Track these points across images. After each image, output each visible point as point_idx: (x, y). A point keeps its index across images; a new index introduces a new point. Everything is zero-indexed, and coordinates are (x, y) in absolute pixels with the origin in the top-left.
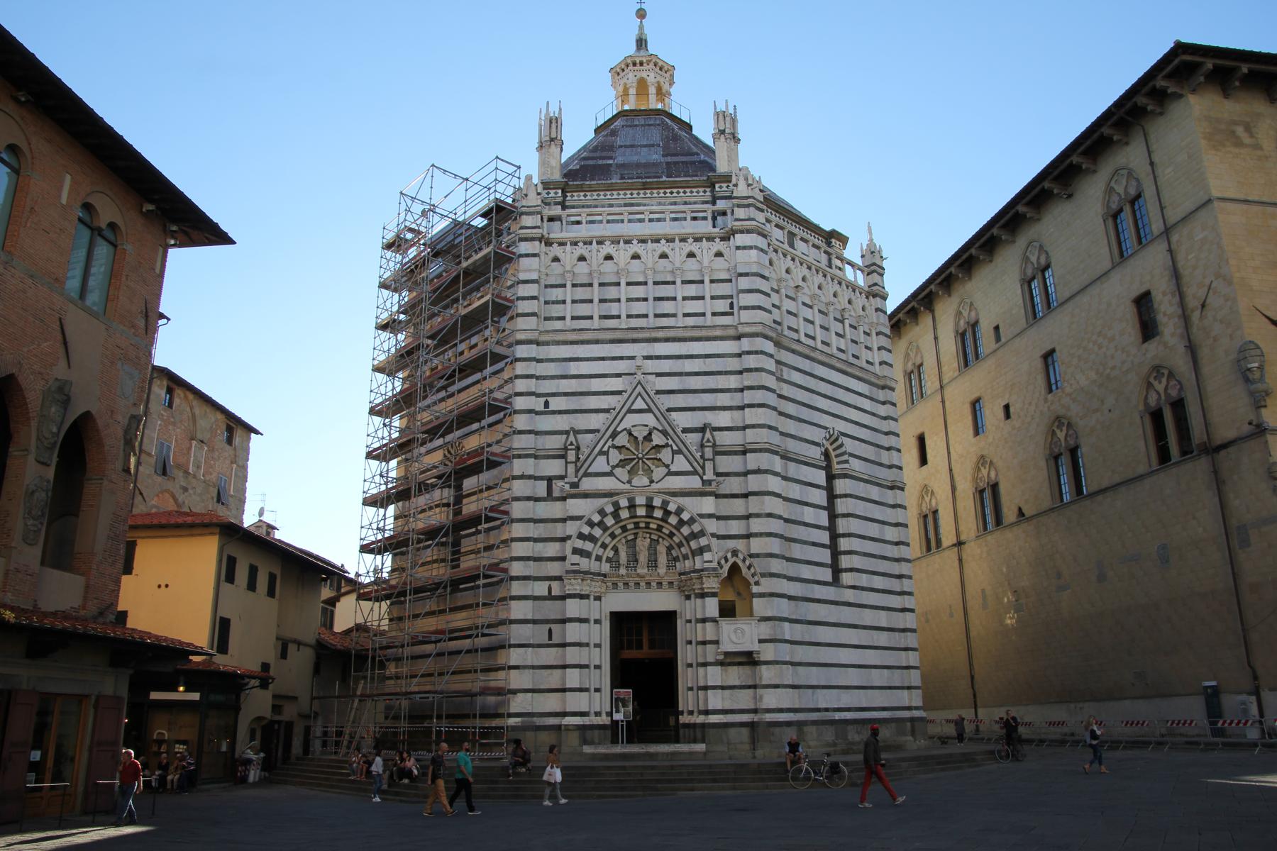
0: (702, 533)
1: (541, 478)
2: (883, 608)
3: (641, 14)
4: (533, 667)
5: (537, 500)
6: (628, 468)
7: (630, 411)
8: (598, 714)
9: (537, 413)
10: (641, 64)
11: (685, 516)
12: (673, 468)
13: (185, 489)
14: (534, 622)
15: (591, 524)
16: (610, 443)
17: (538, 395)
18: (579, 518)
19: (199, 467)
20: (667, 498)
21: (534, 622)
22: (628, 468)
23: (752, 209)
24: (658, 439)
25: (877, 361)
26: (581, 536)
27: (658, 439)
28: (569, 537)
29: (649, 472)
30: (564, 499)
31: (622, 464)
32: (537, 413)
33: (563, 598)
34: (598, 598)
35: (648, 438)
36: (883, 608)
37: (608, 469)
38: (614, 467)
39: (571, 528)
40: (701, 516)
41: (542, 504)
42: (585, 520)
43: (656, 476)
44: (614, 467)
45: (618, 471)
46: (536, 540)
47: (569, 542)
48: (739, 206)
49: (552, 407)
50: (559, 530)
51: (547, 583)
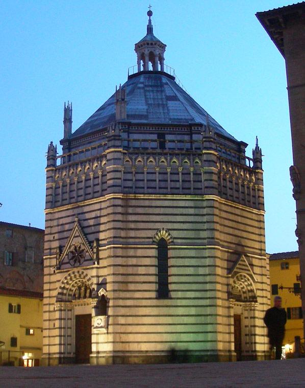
0: (92, 284)
1: (52, 266)
2: (193, 306)
3: (150, 14)
4: (49, 337)
5: (50, 275)
6: (73, 260)
7: (75, 237)
8: (70, 353)
9: (50, 241)
10: (142, 46)
11: (88, 278)
12: (86, 258)
13: (24, 269)
14: (49, 320)
15: (63, 283)
16: (69, 251)
17: (51, 234)
18: (59, 281)
19: (31, 258)
21: (49, 320)
22: (73, 260)
23: (113, 141)
24: (83, 247)
25: (203, 188)
26: (60, 288)
27: (83, 247)
28: (57, 288)
29: (79, 262)
30: (56, 274)
31: (72, 259)
32: (50, 241)
33: (55, 311)
34: (71, 310)
35: (80, 247)
36: (193, 306)
37: (67, 261)
38: (70, 260)
39: (58, 285)
40: (92, 277)
42: (61, 281)
43: (81, 262)
44: (70, 260)
46: (50, 290)
48: (109, 141)
49: (55, 238)
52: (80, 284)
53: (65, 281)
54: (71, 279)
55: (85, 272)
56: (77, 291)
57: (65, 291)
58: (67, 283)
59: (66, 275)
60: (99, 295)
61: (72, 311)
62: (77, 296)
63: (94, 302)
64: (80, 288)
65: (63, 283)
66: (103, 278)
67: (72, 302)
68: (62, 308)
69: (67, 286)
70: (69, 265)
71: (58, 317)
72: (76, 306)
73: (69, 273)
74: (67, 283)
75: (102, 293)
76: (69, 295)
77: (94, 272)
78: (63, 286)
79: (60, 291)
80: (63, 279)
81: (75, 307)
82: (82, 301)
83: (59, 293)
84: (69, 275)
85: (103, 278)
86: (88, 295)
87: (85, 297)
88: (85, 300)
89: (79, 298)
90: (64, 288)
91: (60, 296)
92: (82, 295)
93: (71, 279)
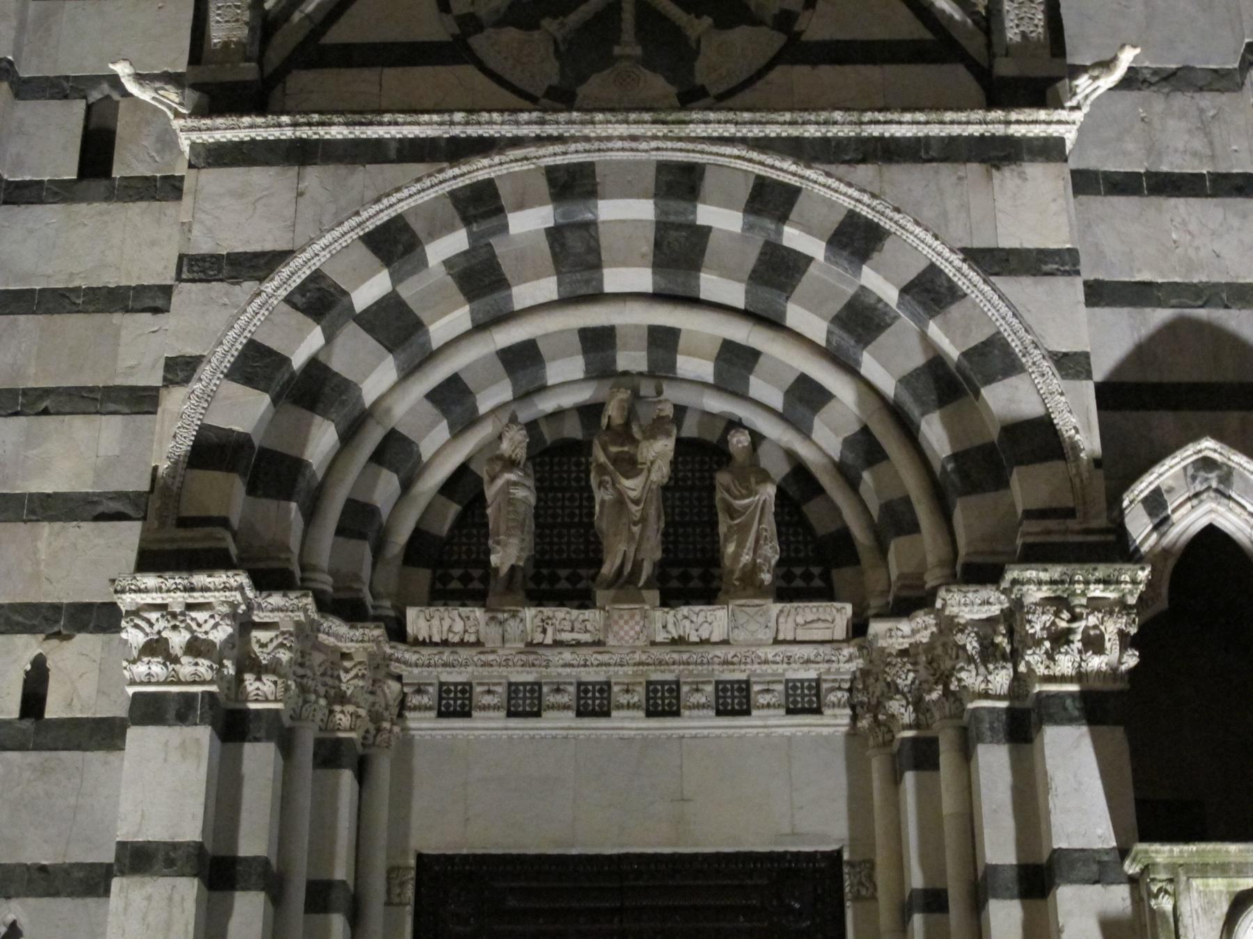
18: (254, 266)
20: (785, 170)
26: (256, 365)
28: (181, 369)
37: (435, 29)
38: (471, 24)
40: (994, 261)
41: (49, 215)
45: (498, 45)
47: (176, 401)
50: (138, 348)
51: (26, 647)
52: (567, 381)
53: (369, 290)
54: (480, 278)
55: (831, 192)
56: (511, 492)
57: (322, 440)
58: (395, 326)
59: (417, 193)
60: (1139, 526)
61: (383, 769)
62: (506, 555)
63: (1090, 629)
64: (560, 460)
65: (319, 300)
66: (1159, 316)
67: (398, 632)
68: (262, 693)
69: (376, 378)
70: (468, 72)
71: (190, 830)
72: (456, 703)
73: (481, 169)
74: (395, 326)
75: (1188, 521)
76: (359, 520)
77: (1031, 208)
78: (305, 344)
79: (246, 411)
80: (328, 249)
81: (422, 724)
82: (630, 635)
83: (212, 450)
84: (481, 205)
85: (1159, 316)
86: (753, 544)
87: (691, 574)
88: (710, 621)
89: (565, 570)
90: (313, 389)
91: (227, 494)
92: (633, 542)
93: (480, 278)
